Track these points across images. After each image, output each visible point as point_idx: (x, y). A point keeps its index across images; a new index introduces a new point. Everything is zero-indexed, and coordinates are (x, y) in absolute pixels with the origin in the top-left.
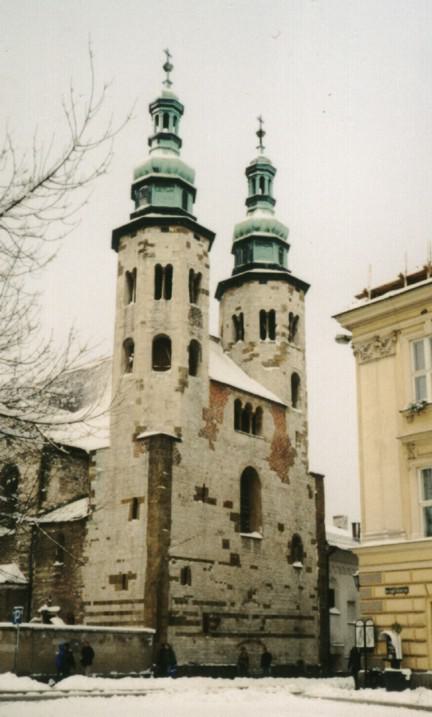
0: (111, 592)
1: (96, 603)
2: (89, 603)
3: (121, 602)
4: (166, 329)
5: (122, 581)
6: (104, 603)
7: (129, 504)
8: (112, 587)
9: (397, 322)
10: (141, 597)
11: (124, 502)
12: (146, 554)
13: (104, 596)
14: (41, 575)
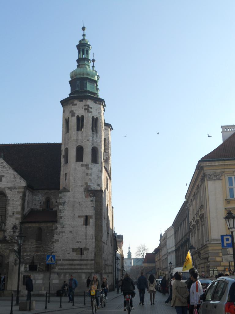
0: (74, 256)
1: (63, 260)
2: (60, 260)
3: (81, 260)
4: (97, 145)
5: (81, 251)
6: (69, 260)
7: (83, 218)
8: (75, 254)
9: (225, 169)
10: (93, 258)
11: (79, 217)
12: (94, 240)
13: (68, 257)
14: (26, 246)
